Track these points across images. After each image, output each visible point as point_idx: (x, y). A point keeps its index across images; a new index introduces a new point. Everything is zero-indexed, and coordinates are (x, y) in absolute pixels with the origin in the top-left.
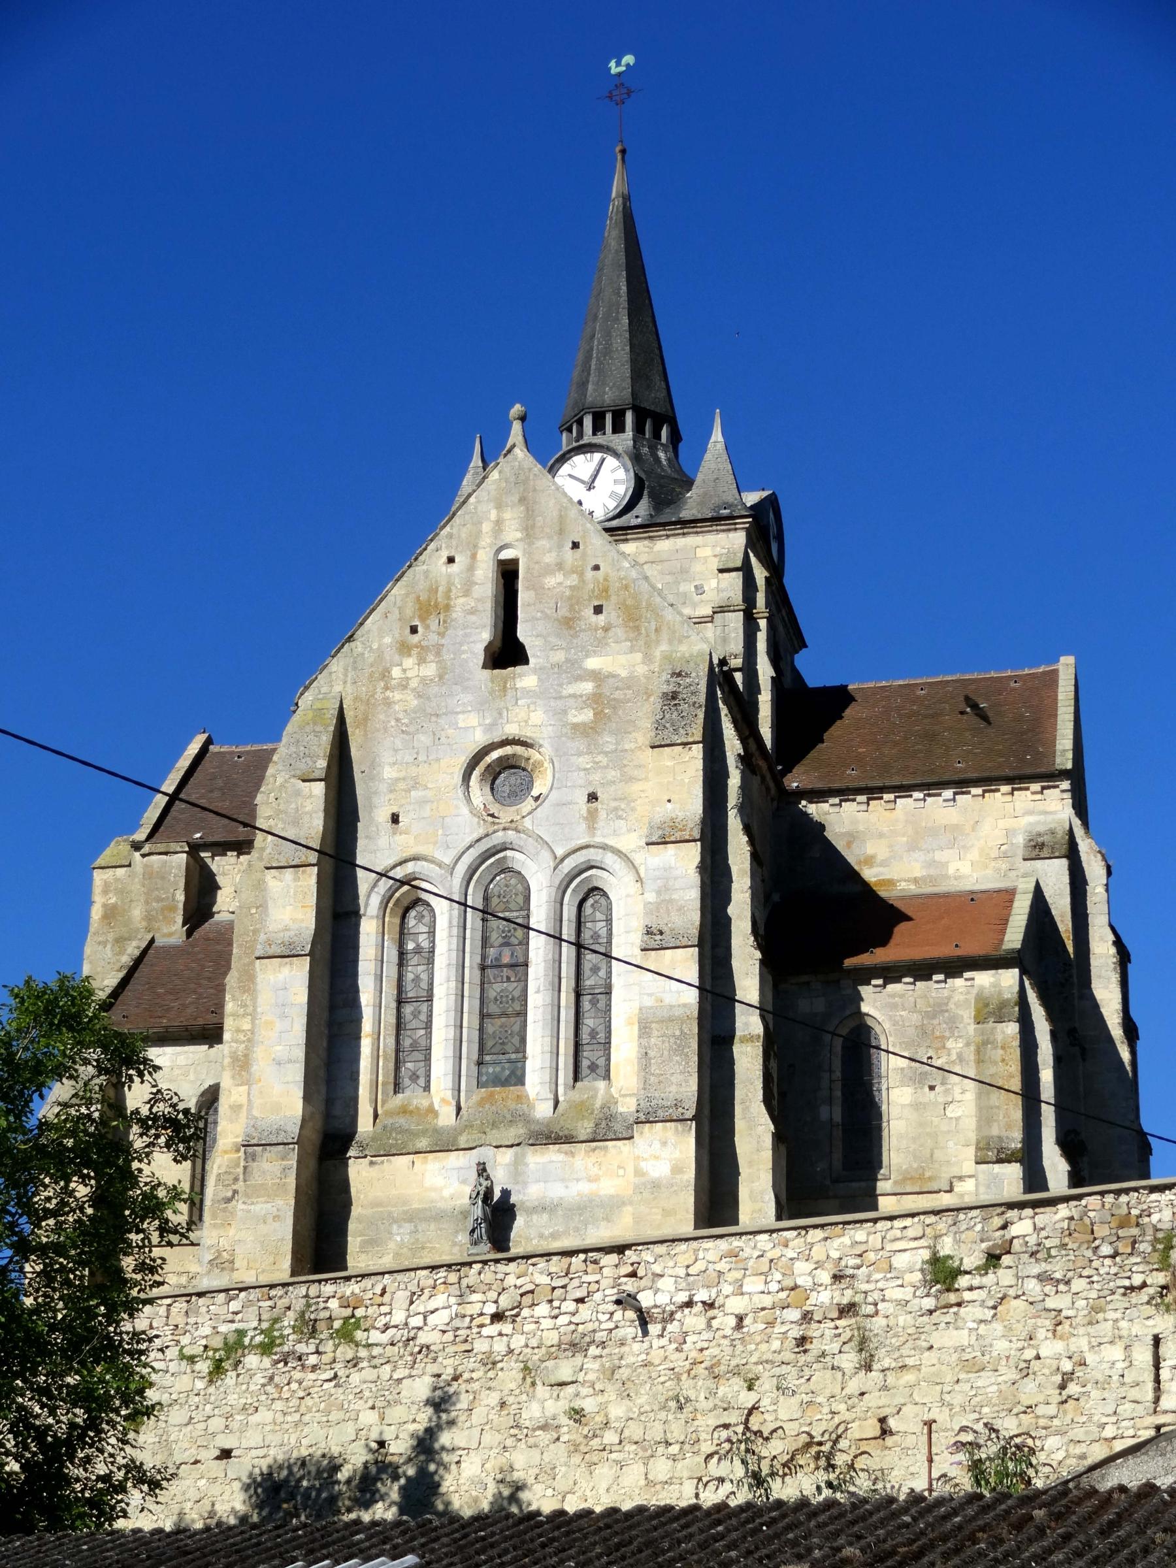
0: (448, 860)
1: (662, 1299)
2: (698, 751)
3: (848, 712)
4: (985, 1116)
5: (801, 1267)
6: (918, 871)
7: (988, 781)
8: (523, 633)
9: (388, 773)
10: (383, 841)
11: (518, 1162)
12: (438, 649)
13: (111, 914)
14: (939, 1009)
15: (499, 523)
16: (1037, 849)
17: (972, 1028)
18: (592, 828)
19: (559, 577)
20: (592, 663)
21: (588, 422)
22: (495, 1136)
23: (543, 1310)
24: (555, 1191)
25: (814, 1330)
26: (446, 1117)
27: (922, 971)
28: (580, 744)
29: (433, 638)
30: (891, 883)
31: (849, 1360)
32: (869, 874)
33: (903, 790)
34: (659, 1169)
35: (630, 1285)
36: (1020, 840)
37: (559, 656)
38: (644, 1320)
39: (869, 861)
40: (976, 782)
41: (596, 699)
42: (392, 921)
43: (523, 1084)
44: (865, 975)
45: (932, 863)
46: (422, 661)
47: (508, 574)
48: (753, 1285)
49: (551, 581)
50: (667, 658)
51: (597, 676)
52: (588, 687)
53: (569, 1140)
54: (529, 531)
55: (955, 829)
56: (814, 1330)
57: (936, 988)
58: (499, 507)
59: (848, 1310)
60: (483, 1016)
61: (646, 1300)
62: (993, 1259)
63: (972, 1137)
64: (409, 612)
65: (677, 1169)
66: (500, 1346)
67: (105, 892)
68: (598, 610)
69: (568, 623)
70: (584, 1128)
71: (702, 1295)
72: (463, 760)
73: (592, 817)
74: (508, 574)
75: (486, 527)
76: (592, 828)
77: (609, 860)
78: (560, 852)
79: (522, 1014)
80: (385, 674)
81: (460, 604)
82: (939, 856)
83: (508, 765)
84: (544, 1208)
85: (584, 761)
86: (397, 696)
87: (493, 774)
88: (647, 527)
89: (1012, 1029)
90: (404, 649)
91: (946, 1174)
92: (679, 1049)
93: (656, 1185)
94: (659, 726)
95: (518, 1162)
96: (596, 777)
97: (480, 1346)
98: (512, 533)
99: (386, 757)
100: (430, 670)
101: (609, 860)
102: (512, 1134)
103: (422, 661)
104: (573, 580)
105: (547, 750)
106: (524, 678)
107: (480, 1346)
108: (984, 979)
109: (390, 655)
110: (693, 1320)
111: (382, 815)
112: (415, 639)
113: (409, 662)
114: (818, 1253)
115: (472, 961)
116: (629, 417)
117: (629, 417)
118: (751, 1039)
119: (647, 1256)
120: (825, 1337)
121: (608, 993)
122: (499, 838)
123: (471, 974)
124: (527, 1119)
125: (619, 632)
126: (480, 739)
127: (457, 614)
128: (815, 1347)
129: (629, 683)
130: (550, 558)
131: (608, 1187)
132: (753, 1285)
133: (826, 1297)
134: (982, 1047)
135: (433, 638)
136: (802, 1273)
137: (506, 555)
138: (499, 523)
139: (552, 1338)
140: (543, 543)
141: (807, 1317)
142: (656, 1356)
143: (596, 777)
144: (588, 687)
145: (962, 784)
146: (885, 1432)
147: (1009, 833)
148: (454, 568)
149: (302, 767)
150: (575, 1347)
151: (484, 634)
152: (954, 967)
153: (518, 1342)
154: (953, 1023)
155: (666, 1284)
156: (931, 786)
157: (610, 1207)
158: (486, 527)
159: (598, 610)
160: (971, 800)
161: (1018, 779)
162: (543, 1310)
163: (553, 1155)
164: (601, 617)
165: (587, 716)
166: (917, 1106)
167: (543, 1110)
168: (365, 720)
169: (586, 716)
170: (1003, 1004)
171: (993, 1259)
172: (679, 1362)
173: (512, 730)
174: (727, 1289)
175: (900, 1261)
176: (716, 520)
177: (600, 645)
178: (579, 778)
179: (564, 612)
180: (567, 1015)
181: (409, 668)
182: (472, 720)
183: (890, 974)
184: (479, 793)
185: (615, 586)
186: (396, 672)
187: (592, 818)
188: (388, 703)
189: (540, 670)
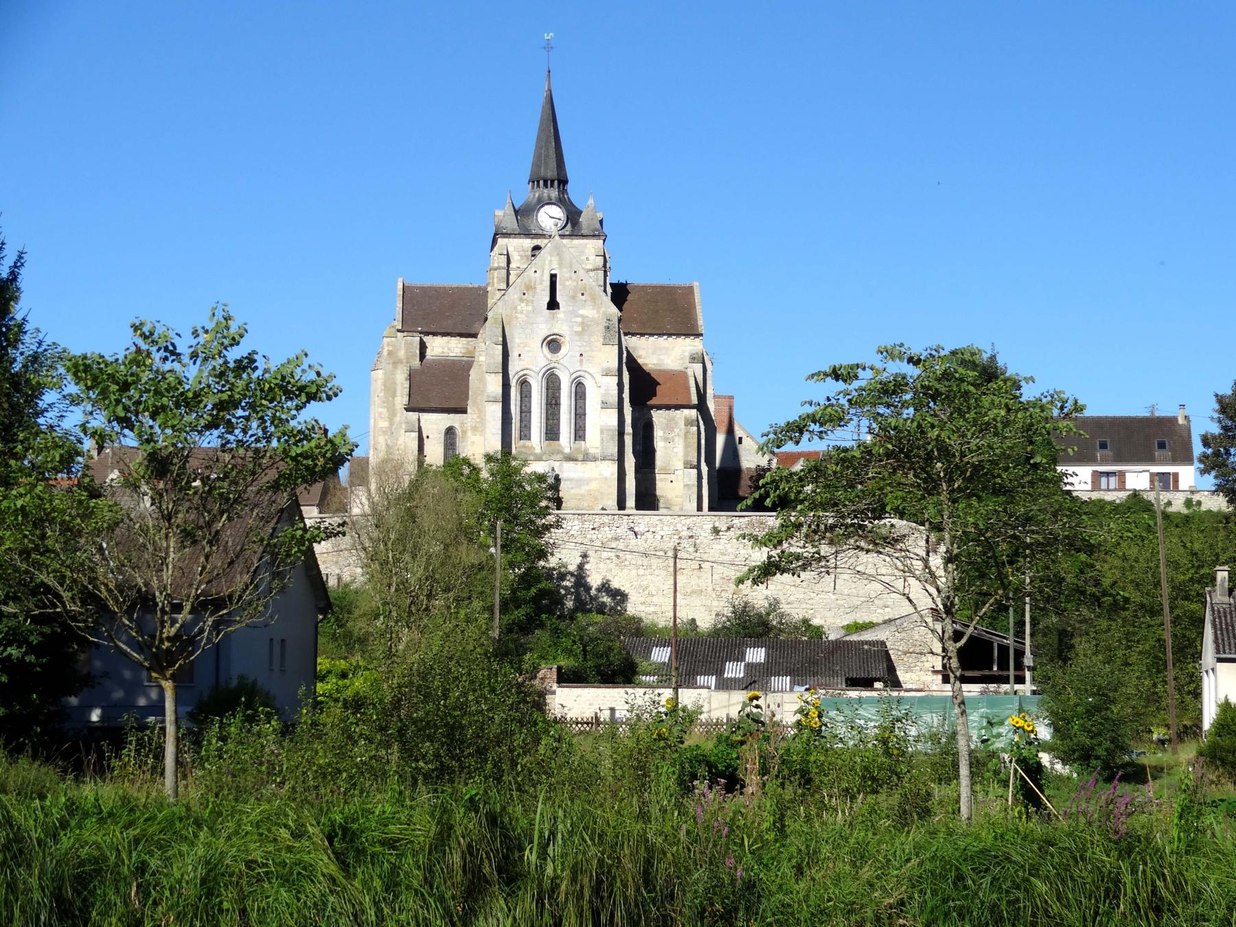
0: (537, 370)
1: (641, 529)
2: (616, 347)
3: (629, 297)
4: (686, 454)
5: (679, 525)
7: (678, 335)
8: (558, 299)
9: (517, 341)
10: (516, 363)
11: (561, 465)
12: (532, 302)
13: (390, 353)
14: (673, 419)
15: (551, 261)
16: (693, 359)
17: (683, 426)
18: (581, 365)
19: (570, 282)
20: (581, 312)
21: (541, 183)
22: (553, 457)
23: (607, 528)
24: (572, 475)
25: (682, 541)
26: (538, 450)
28: (578, 338)
29: (531, 298)
30: (646, 364)
31: (691, 549)
32: (640, 361)
33: (652, 335)
34: (607, 474)
35: (632, 525)
36: (687, 355)
37: (571, 308)
38: (636, 534)
39: (640, 357)
40: (674, 335)
42: (519, 387)
44: (653, 407)
45: (659, 359)
46: (527, 305)
47: (553, 278)
49: (567, 283)
50: (604, 313)
51: (582, 316)
52: (580, 320)
54: (561, 265)
55: (667, 349)
56: (682, 541)
57: (672, 413)
58: (551, 256)
59: (691, 537)
61: (636, 529)
62: (729, 529)
63: (682, 458)
65: (612, 474)
67: (388, 345)
68: (583, 294)
69: (573, 297)
70: (580, 457)
71: (652, 529)
72: (541, 339)
73: (581, 361)
74: (553, 278)
76: (581, 365)
77: (587, 375)
78: (572, 371)
79: (558, 420)
80: (516, 308)
81: (539, 287)
82: (662, 357)
83: (552, 341)
84: (568, 480)
85: (579, 343)
86: (519, 316)
87: (549, 343)
88: (571, 236)
89: (695, 428)
90: (522, 300)
92: (612, 439)
93: (606, 479)
95: (561, 465)
96: (582, 349)
97: (589, 536)
98: (555, 265)
99: (517, 335)
100: (530, 308)
101: (587, 375)
102: (560, 457)
103: (527, 305)
104: (575, 284)
105: (567, 338)
106: (560, 314)
107: (589, 536)
108: (686, 412)
109: (517, 302)
110: (649, 535)
111: (516, 354)
112: (525, 297)
113: (523, 305)
114: (683, 522)
115: (544, 402)
116: (556, 182)
117: (556, 182)
118: (629, 434)
119: (636, 518)
121: (585, 415)
122: (553, 365)
123: (544, 406)
124: (563, 453)
125: (589, 303)
126: (547, 333)
127: (538, 291)
129: (593, 320)
130: (567, 275)
131: (587, 475)
132: (666, 528)
133: (685, 533)
134: (687, 433)
135: (531, 298)
136: (679, 527)
137: (553, 272)
138: (551, 261)
139: (610, 536)
140: (565, 270)
141: (680, 538)
142: (639, 543)
143: (582, 349)
144: (580, 320)
145: (670, 335)
146: (701, 568)
147: (684, 352)
148: (537, 275)
149: (494, 339)
150: (616, 539)
151: (548, 299)
153: (600, 536)
154: (676, 423)
155: (642, 525)
156: (660, 335)
157: (588, 481)
159: (583, 294)
160: (671, 340)
161: (687, 335)
162: (607, 528)
163: (571, 464)
164: (583, 297)
165: (579, 329)
166: (665, 448)
167: (567, 450)
168: (509, 323)
169: (579, 329)
170: (692, 421)
171: (729, 529)
173: (556, 331)
174: (658, 528)
175: (704, 526)
177: (583, 306)
178: (577, 349)
179: (572, 294)
180: (573, 421)
181: (522, 306)
182: (543, 326)
183: (659, 407)
184: (545, 349)
185: (588, 287)
186: (519, 307)
187: (581, 361)
188: (517, 318)
189: (564, 312)
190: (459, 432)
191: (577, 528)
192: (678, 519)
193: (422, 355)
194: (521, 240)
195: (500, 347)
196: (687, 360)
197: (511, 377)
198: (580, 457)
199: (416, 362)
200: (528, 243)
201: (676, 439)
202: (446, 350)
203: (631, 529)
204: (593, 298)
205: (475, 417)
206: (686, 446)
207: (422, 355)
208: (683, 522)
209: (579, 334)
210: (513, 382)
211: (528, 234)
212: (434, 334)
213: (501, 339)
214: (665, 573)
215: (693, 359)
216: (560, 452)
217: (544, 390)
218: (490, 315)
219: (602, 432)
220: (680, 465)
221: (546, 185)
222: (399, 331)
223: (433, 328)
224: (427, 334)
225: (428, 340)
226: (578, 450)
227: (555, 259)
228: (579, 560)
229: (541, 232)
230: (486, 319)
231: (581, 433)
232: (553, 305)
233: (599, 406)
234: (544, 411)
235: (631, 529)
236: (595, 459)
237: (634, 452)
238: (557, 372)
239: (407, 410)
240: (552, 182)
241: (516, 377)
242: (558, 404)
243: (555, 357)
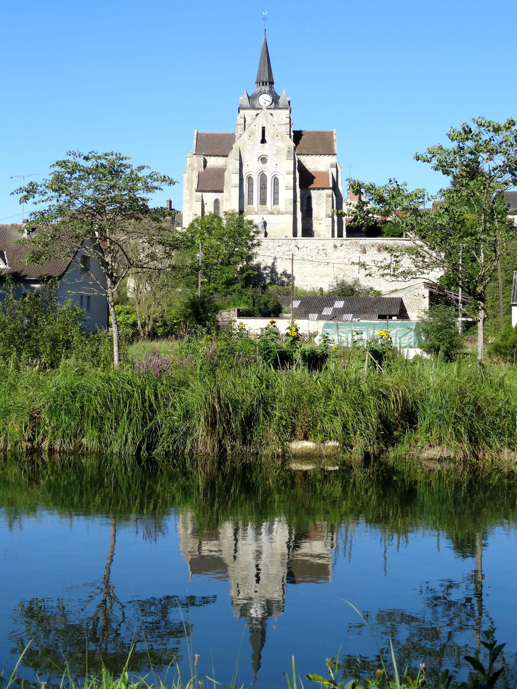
0: (256, 172)
3: (303, 137)
4: (327, 211)
6: (314, 168)
7: (325, 155)
8: (266, 138)
13: (190, 165)
14: (320, 194)
16: (332, 166)
17: (325, 198)
20: (276, 144)
21: (261, 83)
22: (263, 213)
23: (285, 246)
26: (256, 210)
27: (318, 189)
31: (324, 255)
32: (307, 167)
33: (312, 155)
35: (297, 244)
36: (329, 164)
38: (298, 248)
39: (307, 165)
41: (277, 150)
42: (247, 180)
43: (266, 204)
44: (311, 189)
47: (263, 129)
48: (312, 245)
51: (277, 147)
53: (274, 214)
54: (267, 122)
57: (320, 191)
58: (262, 118)
59: (324, 249)
60: (261, 195)
61: (298, 246)
62: (341, 245)
64: (249, 133)
66: (279, 250)
69: (273, 138)
70: (276, 213)
73: (276, 167)
74: (263, 129)
75: (260, 121)
77: (279, 174)
79: (266, 195)
80: (246, 143)
81: (257, 133)
83: (263, 158)
87: (262, 159)
88: (274, 108)
89: (331, 199)
90: (249, 139)
91: (321, 218)
94: (287, 157)
100: (252, 143)
101: (279, 174)
102: (266, 212)
104: (273, 131)
107: (277, 249)
110: (305, 249)
113: (249, 141)
115: (259, 187)
116: (268, 83)
117: (268, 83)
120: (321, 252)
123: (259, 189)
127: (256, 134)
128: (320, 253)
130: (270, 127)
133: (321, 248)
136: (318, 245)
137: (263, 126)
144: (276, 148)
145: (321, 155)
149: (236, 158)
151: (261, 138)
152: (323, 189)
156: (316, 155)
158: (260, 121)
160: (322, 157)
161: (329, 155)
162: (285, 246)
165: (276, 152)
167: (270, 210)
169: (276, 152)
171: (341, 245)
172: (303, 254)
176: (285, 108)
183: (314, 189)
184: (260, 162)
187: (276, 167)
190: (220, 201)
191: (271, 246)
192: (318, 241)
193: (205, 166)
194: (251, 111)
195: (238, 161)
196: (329, 167)
197: (244, 175)
198: (276, 213)
199: (202, 169)
200: (254, 112)
201: (322, 204)
202: (216, 163)
203: (296, 246)
204: (282, 138)
205: (227, 194)
206: (327, 207)
207: (205, 166)
208: (320, 242)
209: (275, 155)
210: (245, 178)
211: (254, 108)
212: (210, 156)
213: (239, 158)
214: (311, 266)
215: (332, 166)
216: (266, 210)
217: (259, 181)
218: (234, 146)
219: (286, 201)
220: (324, 216)
221: (263, 85)
222: (194, 154)
223: (210, 153)
224: (207, 156)
225: (207, 158)
226: (275, 209)
227: (264, 120)
228: (272, 261)
229: (260, 107)
230: (232, 148)
231: (277, 201)
232: (263, 141)
233: (285, 188)
234: (259, 192)
235: (296, 246)
236: (283, 214)
237: (302, 210)
238: (265, 173)
239: (197, 191)
240: (266, 83)
241: (246, 176)
242: (266, 188)
243: (264, 166)
